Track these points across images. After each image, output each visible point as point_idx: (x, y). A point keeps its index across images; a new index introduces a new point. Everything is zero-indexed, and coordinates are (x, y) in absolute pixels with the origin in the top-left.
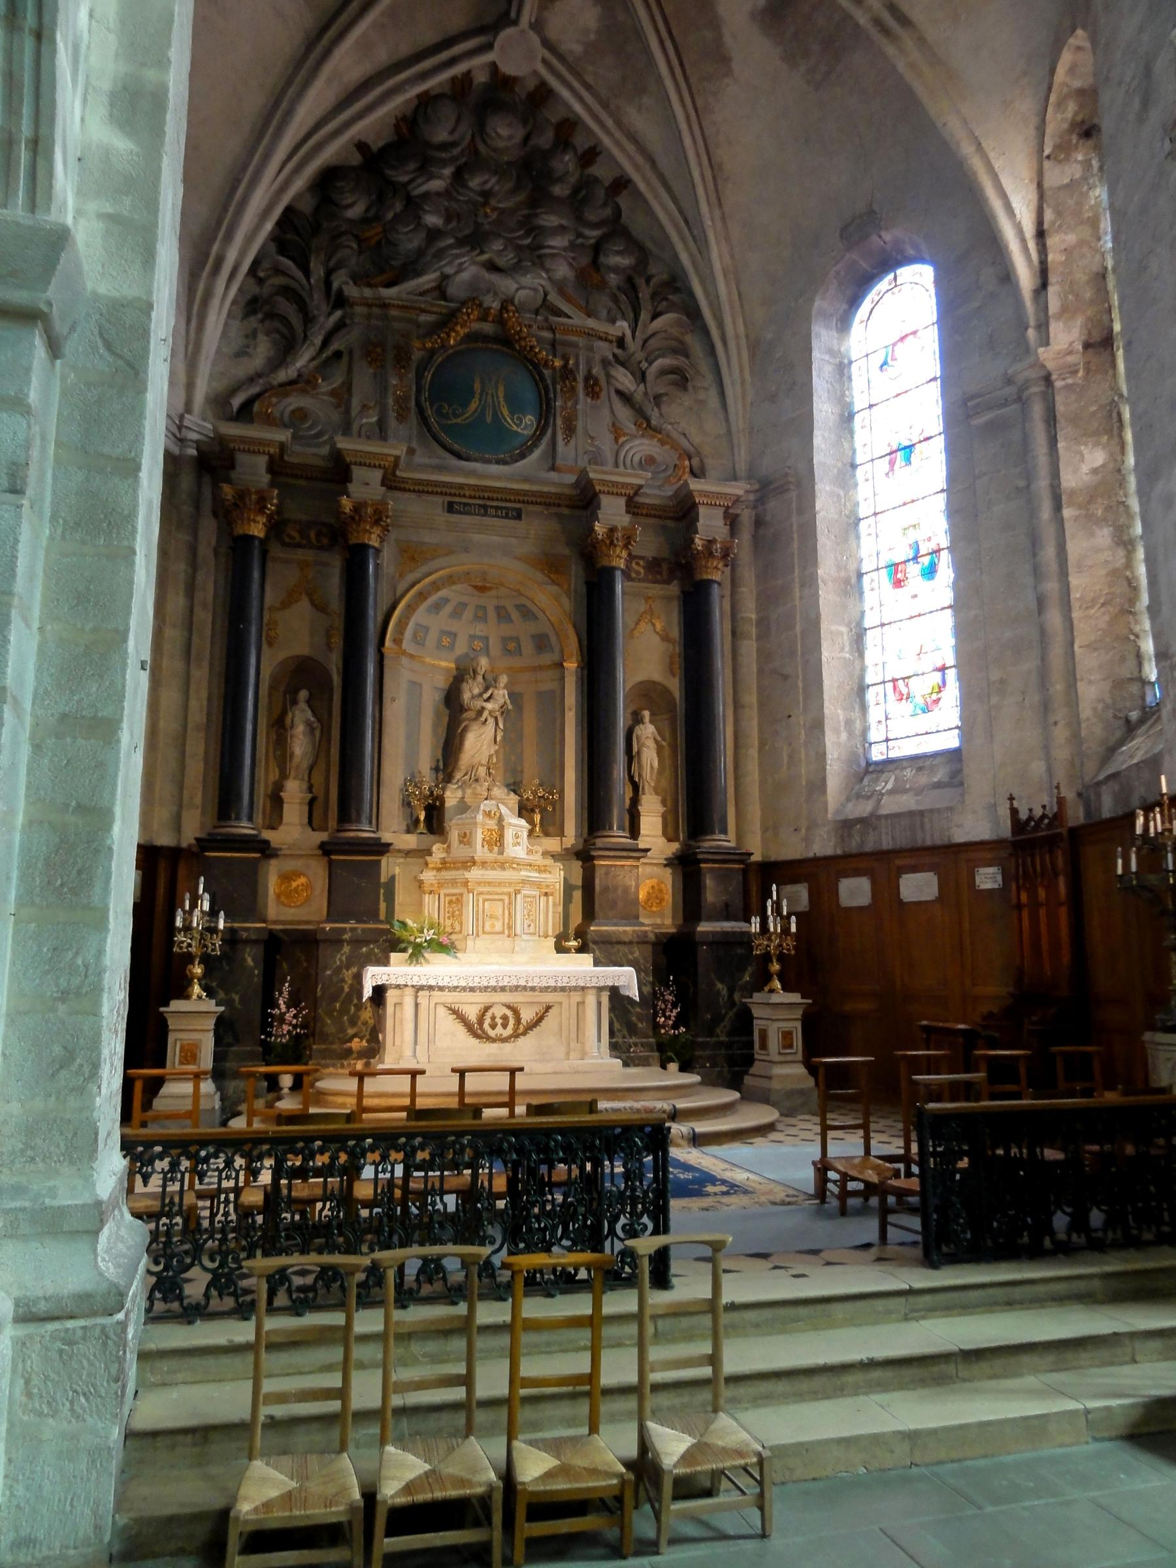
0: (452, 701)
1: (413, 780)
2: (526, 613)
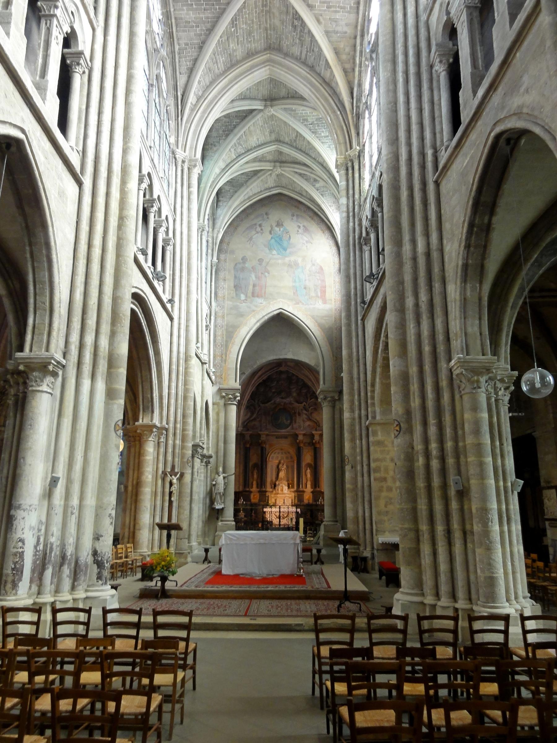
0: (278, 467)
1: (272, 481)
2: (289, 453)
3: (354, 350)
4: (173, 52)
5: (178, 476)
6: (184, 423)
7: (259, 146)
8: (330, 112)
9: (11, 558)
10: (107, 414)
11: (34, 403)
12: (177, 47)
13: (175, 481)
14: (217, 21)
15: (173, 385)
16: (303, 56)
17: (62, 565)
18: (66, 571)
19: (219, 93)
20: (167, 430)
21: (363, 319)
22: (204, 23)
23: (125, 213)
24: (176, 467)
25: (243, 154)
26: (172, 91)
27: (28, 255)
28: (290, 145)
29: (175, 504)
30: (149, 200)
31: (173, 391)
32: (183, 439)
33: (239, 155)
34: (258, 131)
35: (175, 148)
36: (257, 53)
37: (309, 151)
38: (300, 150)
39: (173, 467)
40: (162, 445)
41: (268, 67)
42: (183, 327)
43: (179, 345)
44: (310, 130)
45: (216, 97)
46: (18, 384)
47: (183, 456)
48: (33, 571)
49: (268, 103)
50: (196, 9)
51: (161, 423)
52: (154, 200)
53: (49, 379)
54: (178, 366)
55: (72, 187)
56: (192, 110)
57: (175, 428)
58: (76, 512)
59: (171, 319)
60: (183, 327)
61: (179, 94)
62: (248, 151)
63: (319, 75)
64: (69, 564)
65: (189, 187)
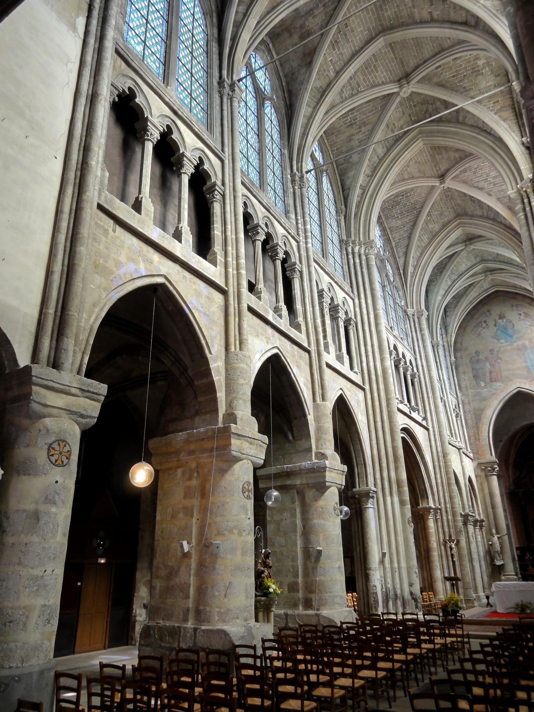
4: (392, 248)
5: (455, 542)
6: (452, 503)
7: (469, 269)
8: (516, 248)
9: (372, 595)
10: (403, 515)
11: (366, 514)
12: (393, 244)
13: (453, 546)
14: (417, 219)
15: (438, 476)
16: (485, 214)
17: (396, 599)
18: (399, 603)
19: (428, 258)
20: (440, 509)
22: (408, 223)
23: (389, 396)
24: (452, 535)
26: (396, 271)
27: (349, 439)
28: (494, 261)
29: (457, 563)
30: (397, 360)
31: (439, 481)
32: (454, 515)
34: (465, 261)
35: (406, 308)
36: (450, 222)
37: (510, 262)
38: (504, 262)
39: (450, 536)
40: (439, 521)
41: (460, 229)
42: (437, 433)
43: (436, 447)
45: (426, 261)
46: (355, 503)
47: (456, 527)
48: (383, 602)
49: (468, 243)
50: (401, 218)
51: (435, 505)
52: (400, 359)
53: (371, 500)
55: (361, 394)
56: (412, 277)
57: (446, 507)
58: (397, 570)
59: (427, 429)
60: (437, 433)
61: (401, 271)
62: (461, 275)
63: (501, 223)
64: (400, 599)
65: (421, 331)
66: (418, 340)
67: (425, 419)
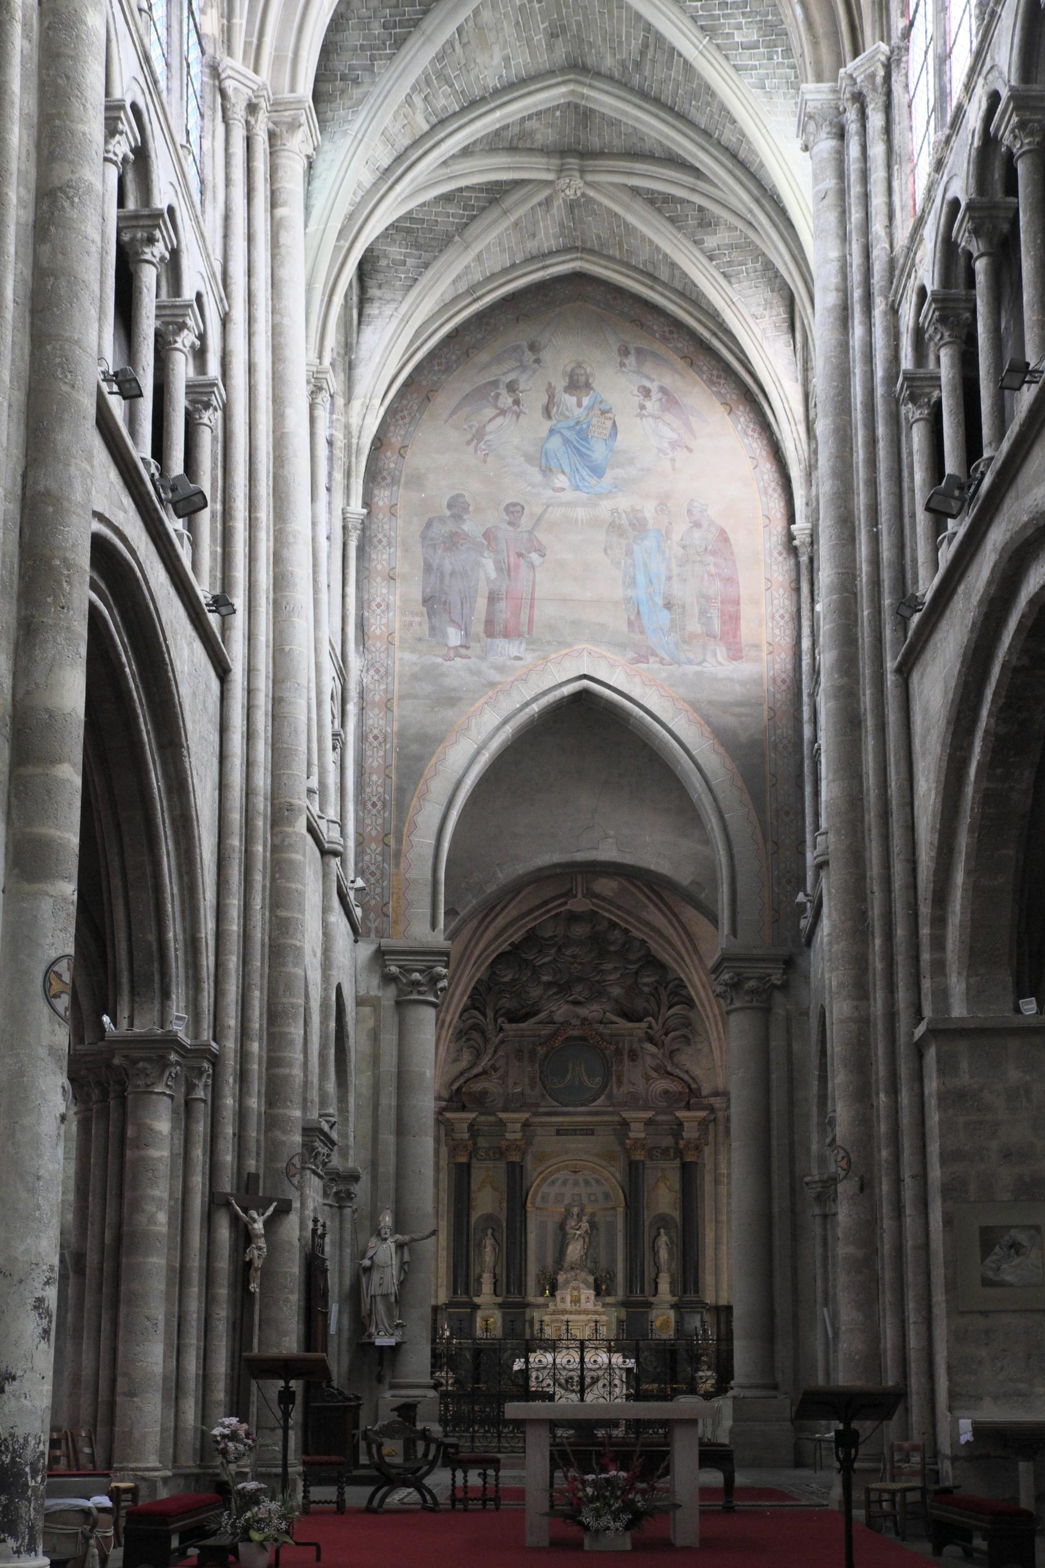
3: (871, 781)
7: (511, 86)
15: (234, 903)
21: (905, 670)
25: (455, 114)
28: (621, 83)
31: (234, 927)
33: (442, 122)
34: (508, 29)
37: (684, 102)
38: (657, 101)
43: (249, 764)
44: (694, 19)
54: (248, 839)
59: (223, 672)
62: (473, 104)
66: (250, 239)
67: (222, 603)
